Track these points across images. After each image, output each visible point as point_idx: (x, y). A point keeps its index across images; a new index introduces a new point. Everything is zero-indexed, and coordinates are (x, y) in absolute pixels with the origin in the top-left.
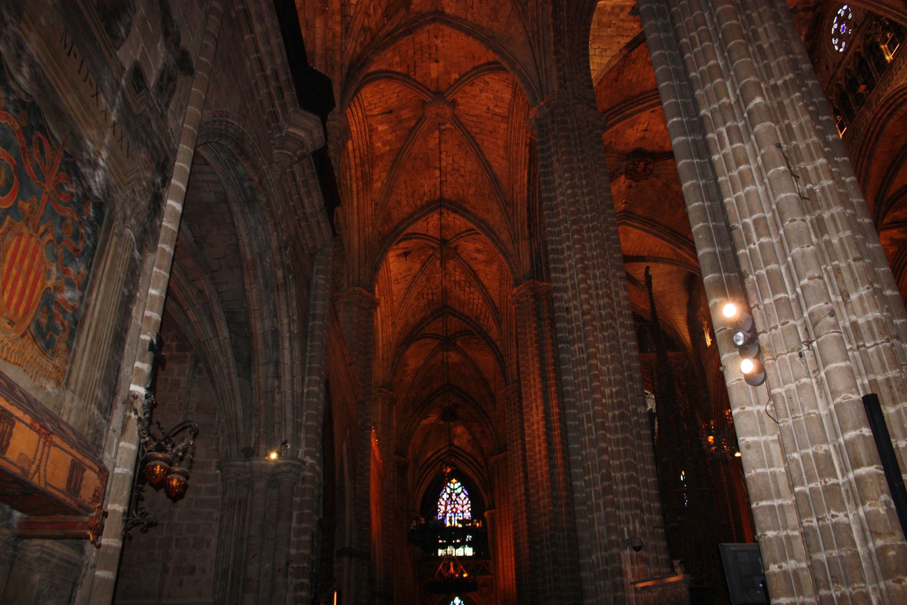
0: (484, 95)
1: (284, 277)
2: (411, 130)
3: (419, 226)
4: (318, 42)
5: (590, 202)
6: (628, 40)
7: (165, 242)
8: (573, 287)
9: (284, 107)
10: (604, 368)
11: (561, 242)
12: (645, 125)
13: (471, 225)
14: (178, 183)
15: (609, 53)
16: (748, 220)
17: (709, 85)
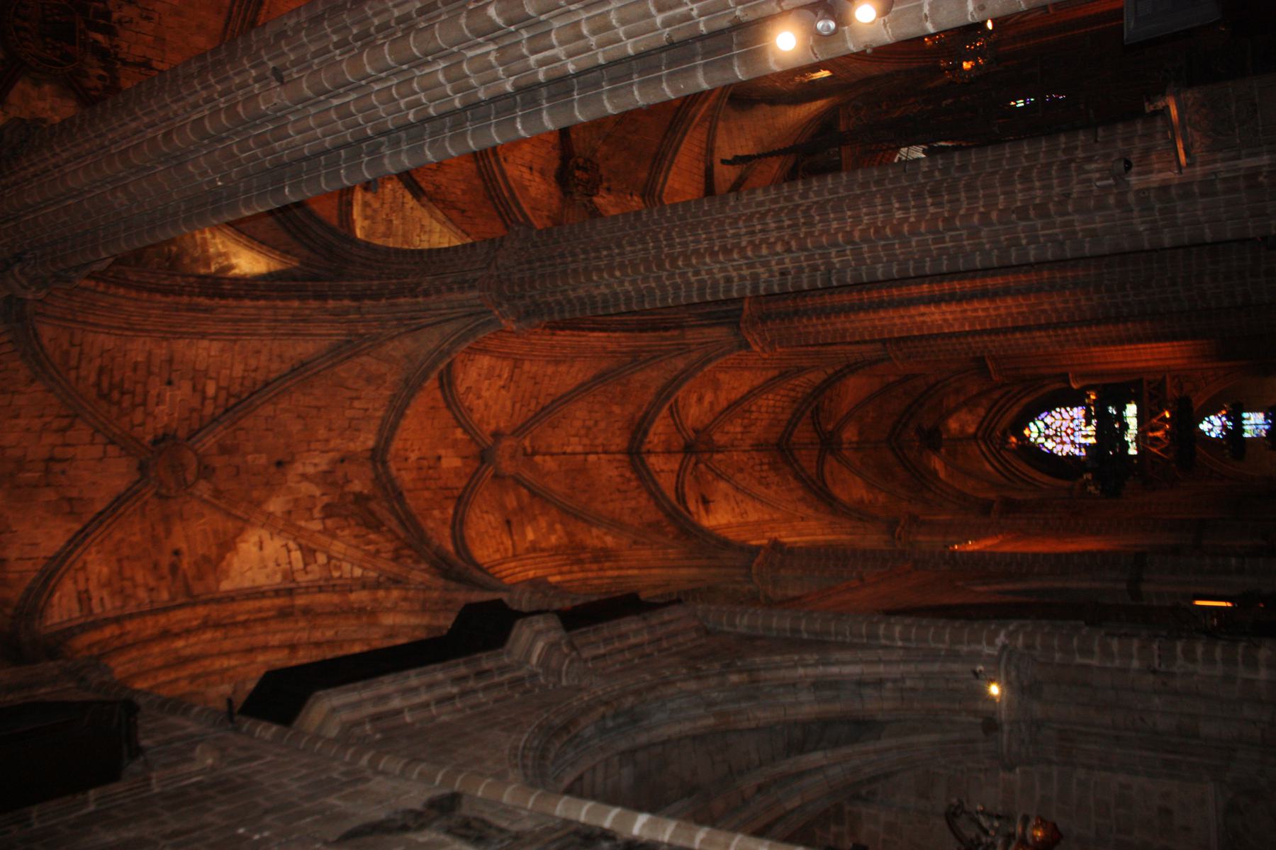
0: (486, 394)
1: (740, 671)
2: (533, 494)
3: (667, 483)
4: (414, 621)
5: (631, 244)
6: (409, 196)
7: (692, 838)
8: (751, 266)
9: (503, 670)
10: (866, 219)
11: (689, 284)
12: (524, 169)
13: (665, 411)
14: (610, 818)
15: (427, 221)
16: (659, 19)
17: (473, 81)
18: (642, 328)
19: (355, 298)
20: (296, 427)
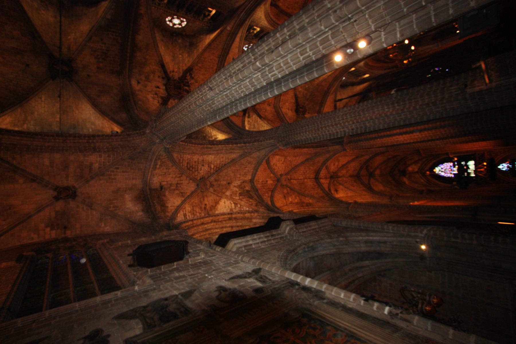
0: (278, 165)
1: (343, 237)
2: (291, 189)
3: (326, 186)
4: (260, 221)
5: (311, 125)
7: (322, 287)
8: (343, 128)
9: (278, 234)
10: (376, 112)
11: (326, 134)
13: (324, 168)
14: (299, 279)
16: (301, 58)
17: (256, 84)
18: (317, 147)
19: (244, 143)
20: (232, 175)
